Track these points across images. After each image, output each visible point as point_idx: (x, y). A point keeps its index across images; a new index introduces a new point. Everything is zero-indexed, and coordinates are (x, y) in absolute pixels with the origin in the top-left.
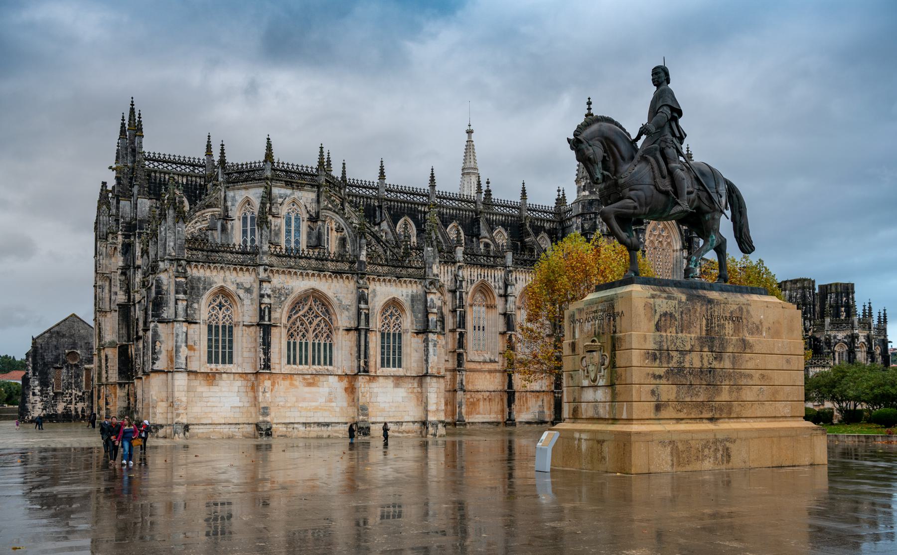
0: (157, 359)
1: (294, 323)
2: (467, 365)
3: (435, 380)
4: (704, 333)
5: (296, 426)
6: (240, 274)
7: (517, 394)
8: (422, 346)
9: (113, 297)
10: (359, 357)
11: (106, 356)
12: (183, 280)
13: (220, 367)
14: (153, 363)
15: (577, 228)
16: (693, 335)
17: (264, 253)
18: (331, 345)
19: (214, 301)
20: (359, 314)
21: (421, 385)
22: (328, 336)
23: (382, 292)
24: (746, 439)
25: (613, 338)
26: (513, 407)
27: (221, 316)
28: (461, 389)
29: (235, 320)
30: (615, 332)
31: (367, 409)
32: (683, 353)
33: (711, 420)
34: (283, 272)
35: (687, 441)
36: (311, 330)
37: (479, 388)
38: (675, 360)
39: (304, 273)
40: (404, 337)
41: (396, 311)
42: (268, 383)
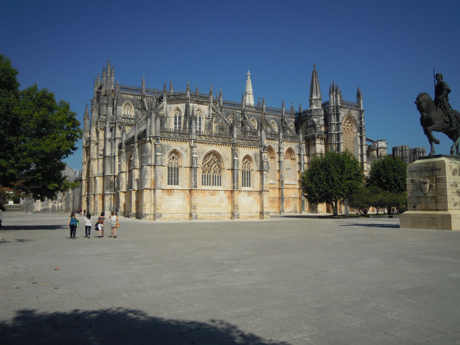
0: (146, 183)
1: (205, 166)
3: (266, 192)
6: (183, 143)
12: (159, 146)
13: (174, 187)
15: (310, 122)
17: (194, 134)
23: (243, 152)
27: (173, 163)
29: (180, 164)
34: (201, 143)
36: (212, 169)
39: (210, 143)
40: (251, 173)
42: (195, 194)
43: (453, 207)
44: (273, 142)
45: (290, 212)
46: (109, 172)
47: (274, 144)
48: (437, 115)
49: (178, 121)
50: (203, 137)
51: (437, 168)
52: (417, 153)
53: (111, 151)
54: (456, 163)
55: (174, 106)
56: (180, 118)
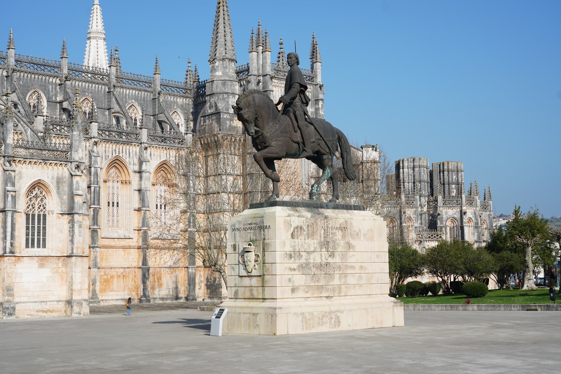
2: (101, 242)
3: (79, 259)
4: (322, 239)
7: (151, 271)
10: (5, 238)
15: (211, 107)
16: (315, 241)
20: (5, 197)
24: (350, 310)
25: (263, 243)
26: (148, 283)
28: (95, 266)
30: (264, 239)
31: (13, 290)
32: (308, 252)
33: (327, 297)
35: (312, 313)
38: (304, 257)
41: (41, 193)
43: (288, 293)
47: (130, 154)
51: (265, 225)
52: (446, 173)
54: (303, 217)
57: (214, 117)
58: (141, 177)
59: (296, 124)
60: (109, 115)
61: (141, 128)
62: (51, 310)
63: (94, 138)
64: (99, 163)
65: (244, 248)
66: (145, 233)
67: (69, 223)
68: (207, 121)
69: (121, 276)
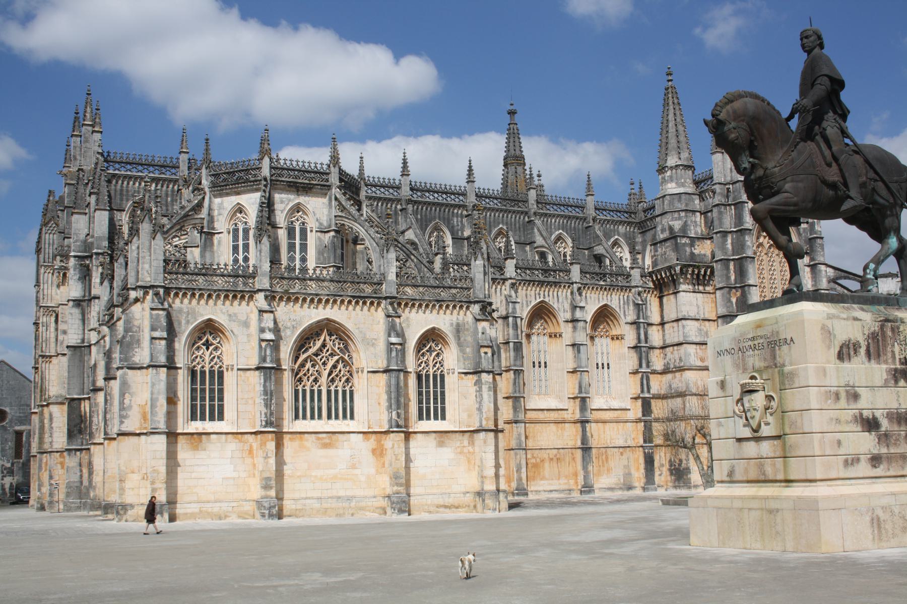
0: (126, 417)
1: (303, 365)
5: (308, 501)
7: (594, 451)
8: (473, 390)
9: (60, 337)
11: (51, 415)
12: (161, 312)
13: (208, 426)
14: (122, 422)
15: (663, 231)
16: (884, 366)
17: (263, 275)
18: (352, 393)
19: (200, 339)
20: (389, 351)
21: (472, 443)
22: (347, 381)
26: (590, 468)
27: (207, 359)
37: (544, 444)
39: (315, 300)
44: (553, 291)
45: (611, 489)
46: (77, 390)
48: (792, 161)
49: (241, 243)
50: (313, 284)
51: (782, 337)
53: (81, 332)
54: (856, 319)
55: (230, 202)
56: (246, 231)
57: (668, 244)
58: (575, 328)
59: (827, 153)
60: (531, 251)
61: (572, 264)
62: (456, 505)
63: (511, 278)
64: (518, 311)
65: (743, 386)
66: (583, 400)
67: (475, 385)
68: (659, 250)
69: (555, 459)
